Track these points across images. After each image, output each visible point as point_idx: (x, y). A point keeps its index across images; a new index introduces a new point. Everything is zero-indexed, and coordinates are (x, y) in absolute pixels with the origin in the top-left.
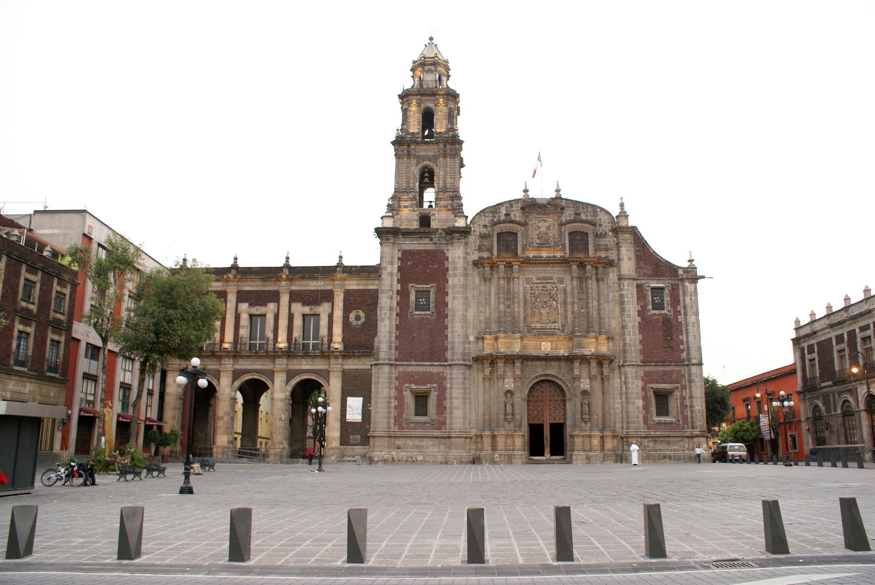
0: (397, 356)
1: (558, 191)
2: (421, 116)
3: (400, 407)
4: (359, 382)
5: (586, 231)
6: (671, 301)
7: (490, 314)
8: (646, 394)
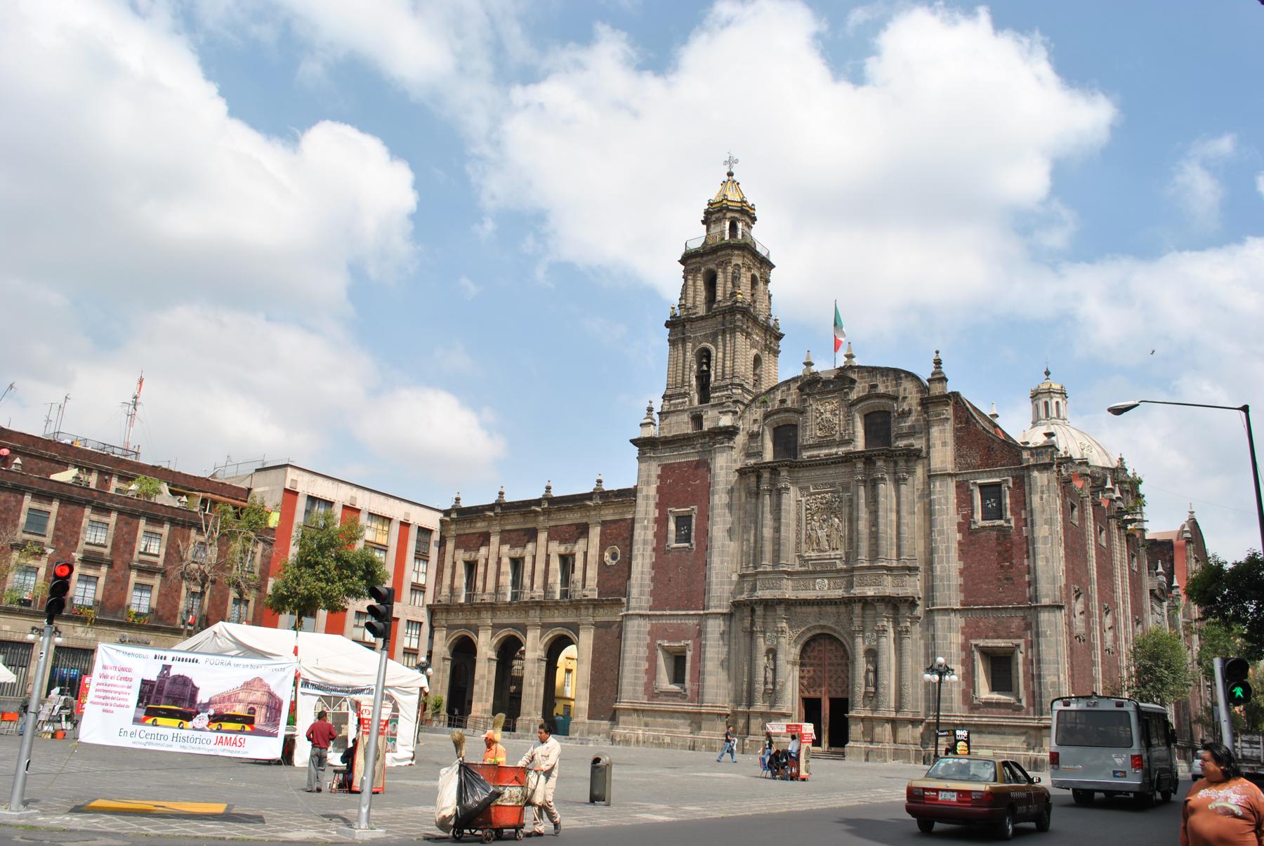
3: (652, 672)
5: (887, 409)
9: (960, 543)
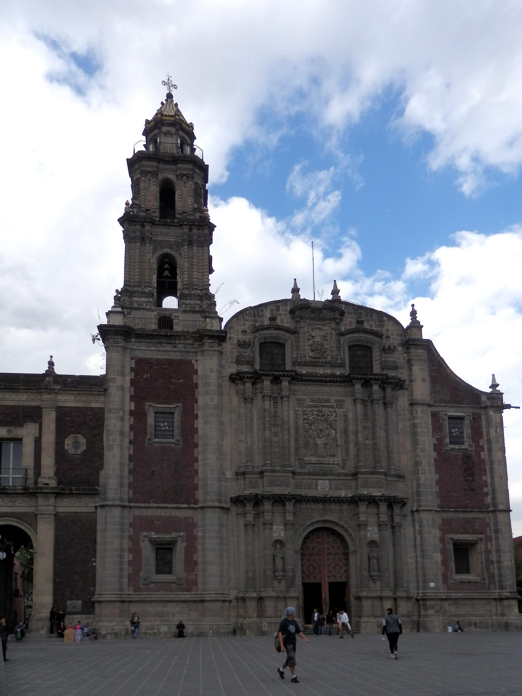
0: (131, 496)
2: (158, 189)
4: (79, 530)
5: (369, 345)
6: (472, 433)
7: (252, 444)
8: (444, 547)
9: (435, 460)
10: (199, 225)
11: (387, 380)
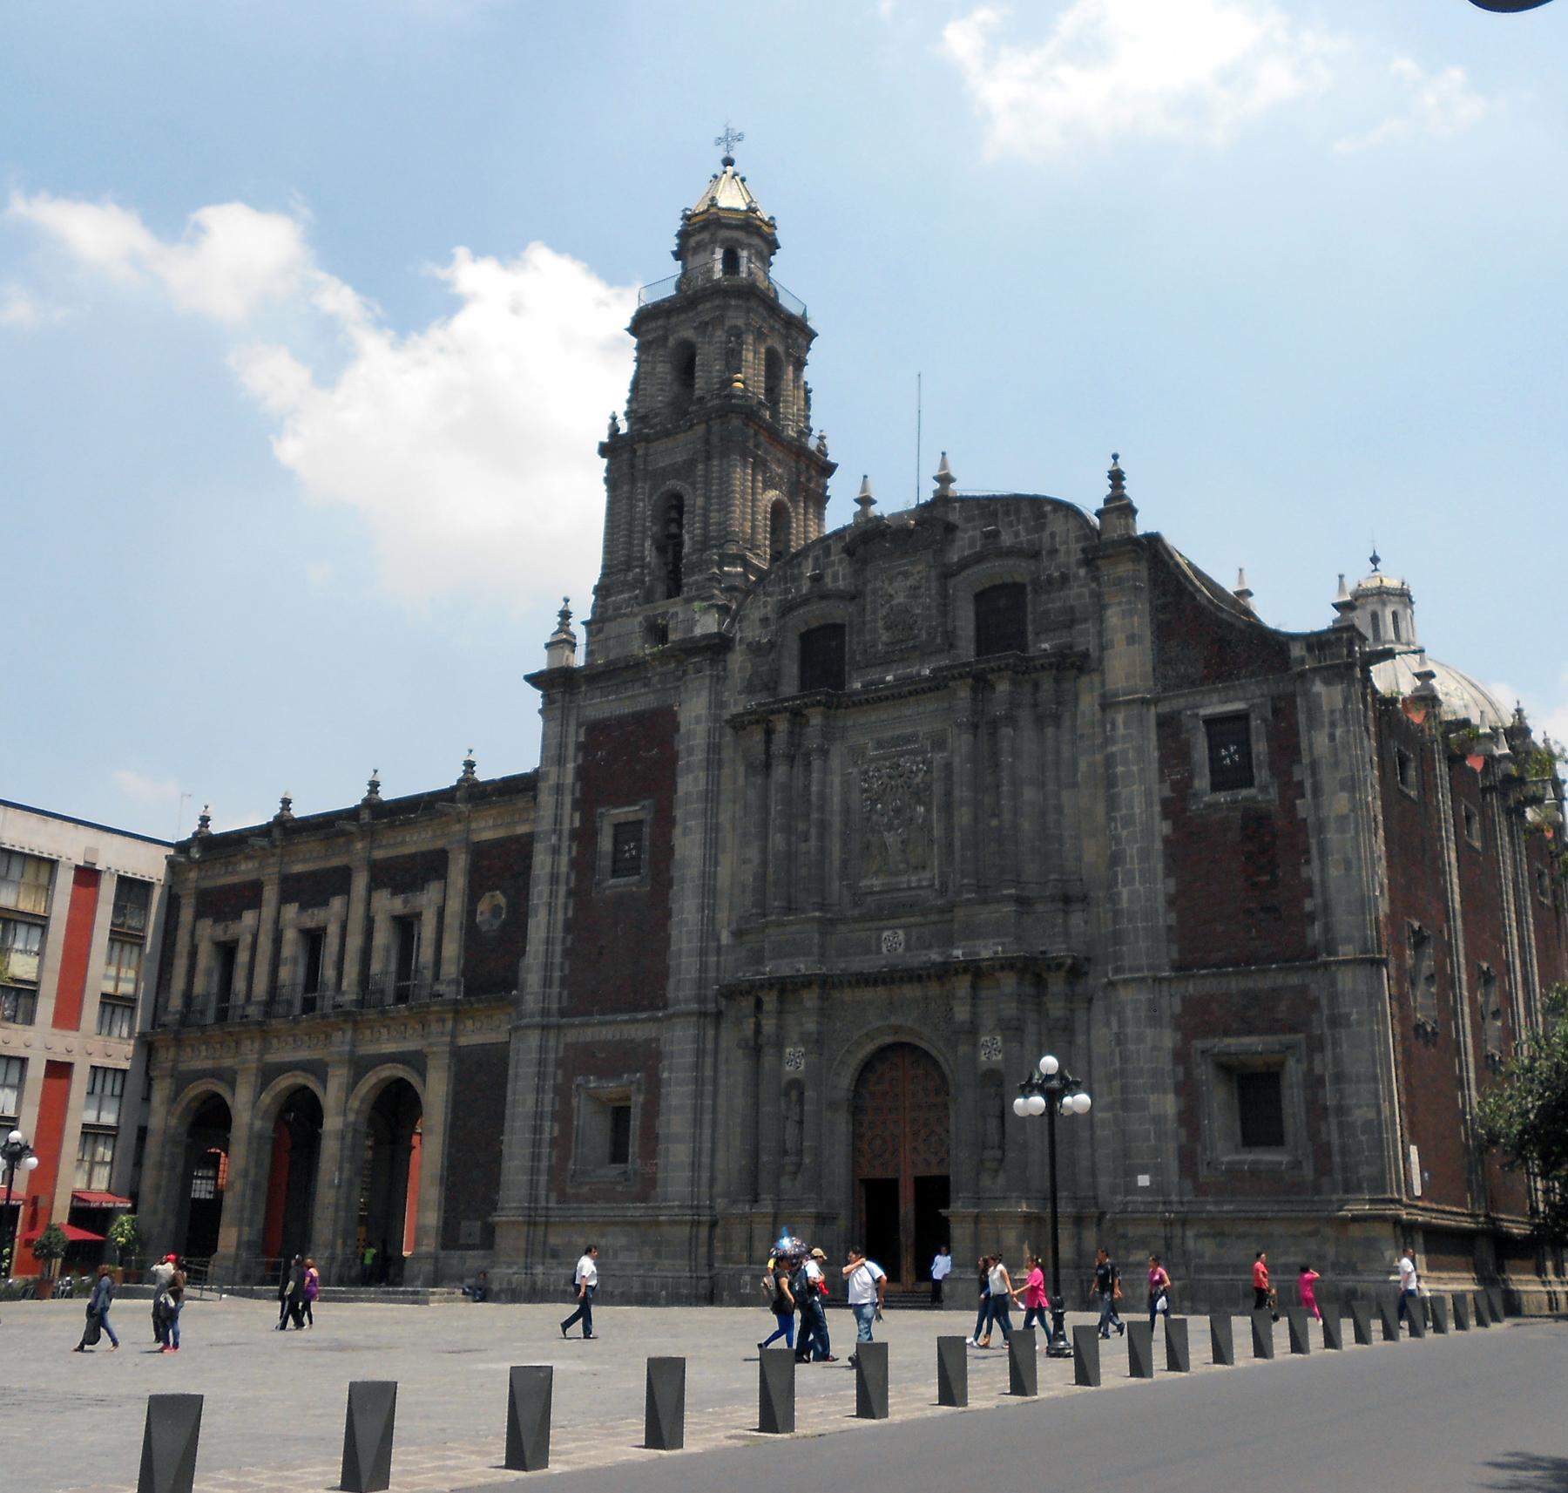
0: (565, 1004)
1: (945, 479)
3: (562, 1144)
6: (1271, 753)
8: (1188, 1074)
9: (1167, 841)
10: (720, 417)
11: (1031, 663)
